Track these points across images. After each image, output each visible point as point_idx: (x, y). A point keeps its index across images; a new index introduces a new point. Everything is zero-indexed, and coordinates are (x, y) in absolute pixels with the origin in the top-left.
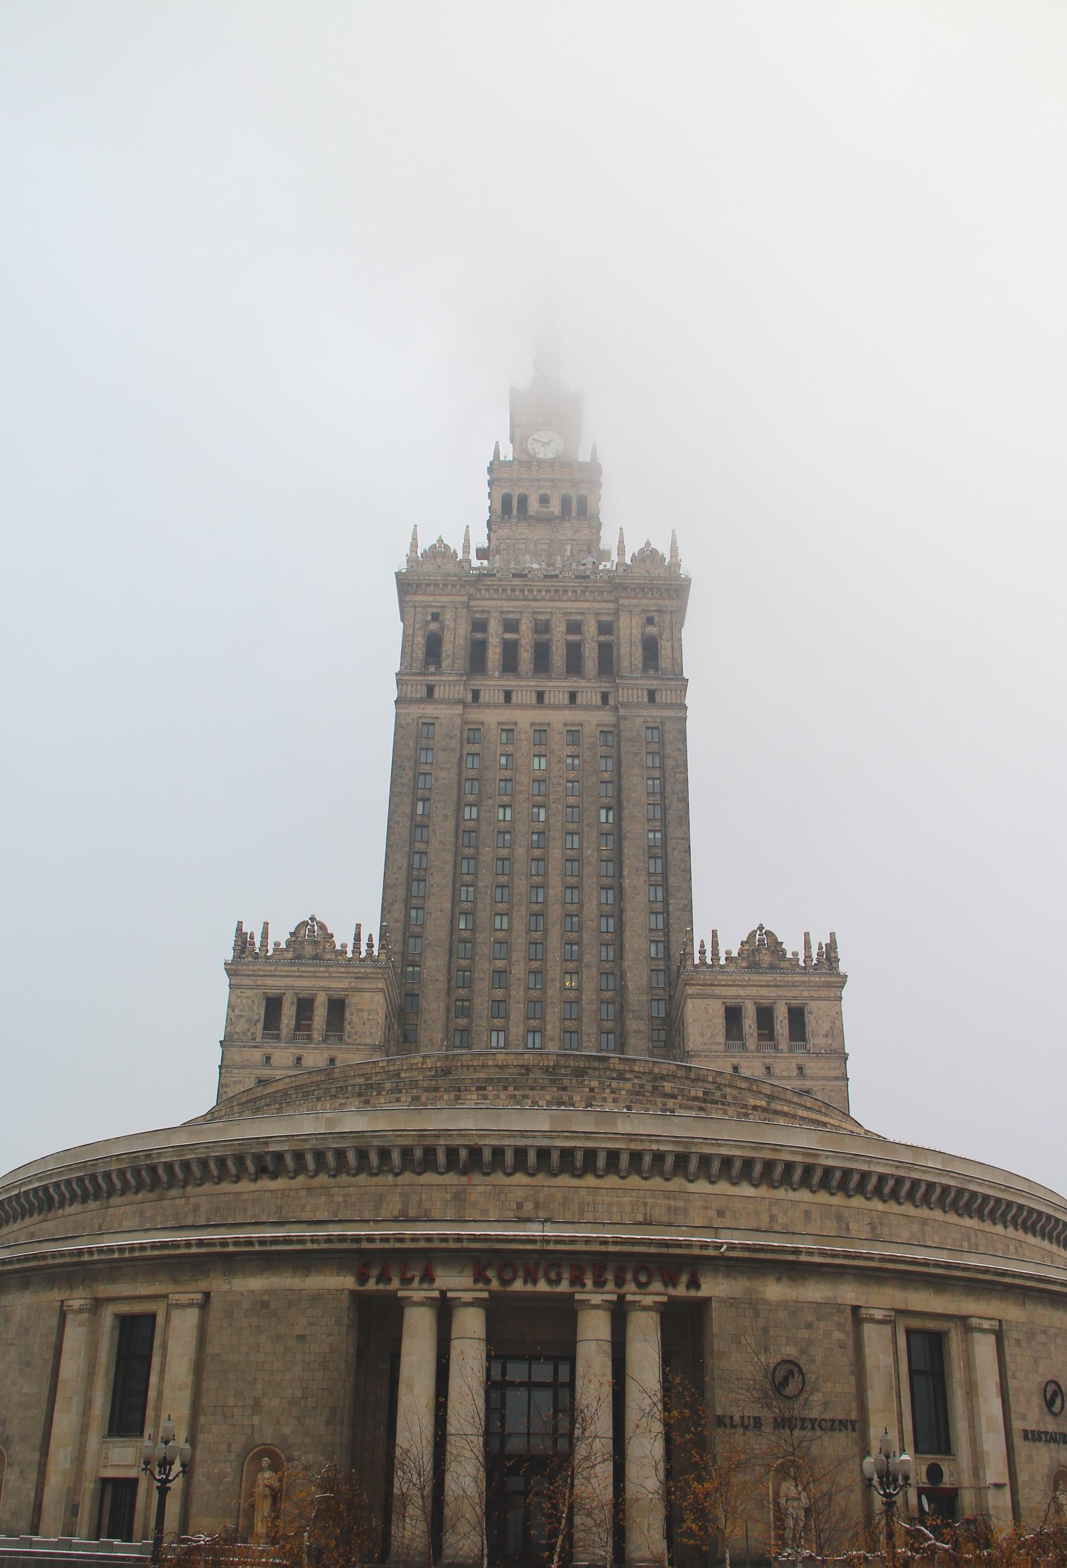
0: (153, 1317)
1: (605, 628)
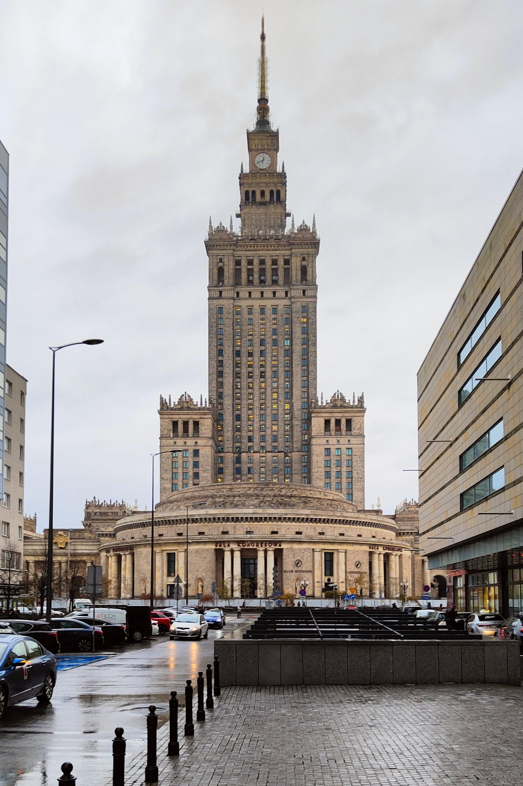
1: (287, 262)
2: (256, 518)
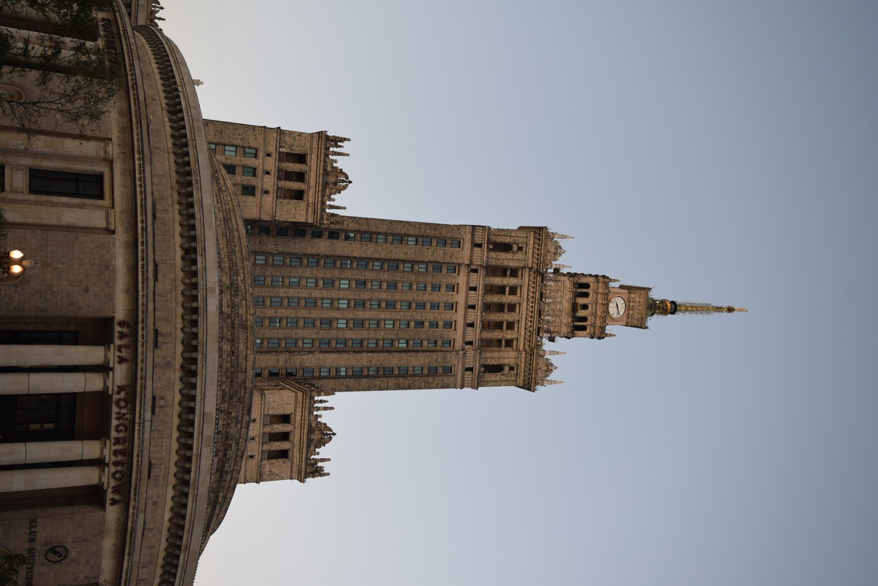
0: (101, 197)
1: (509, 343)
2: (192, 423)
